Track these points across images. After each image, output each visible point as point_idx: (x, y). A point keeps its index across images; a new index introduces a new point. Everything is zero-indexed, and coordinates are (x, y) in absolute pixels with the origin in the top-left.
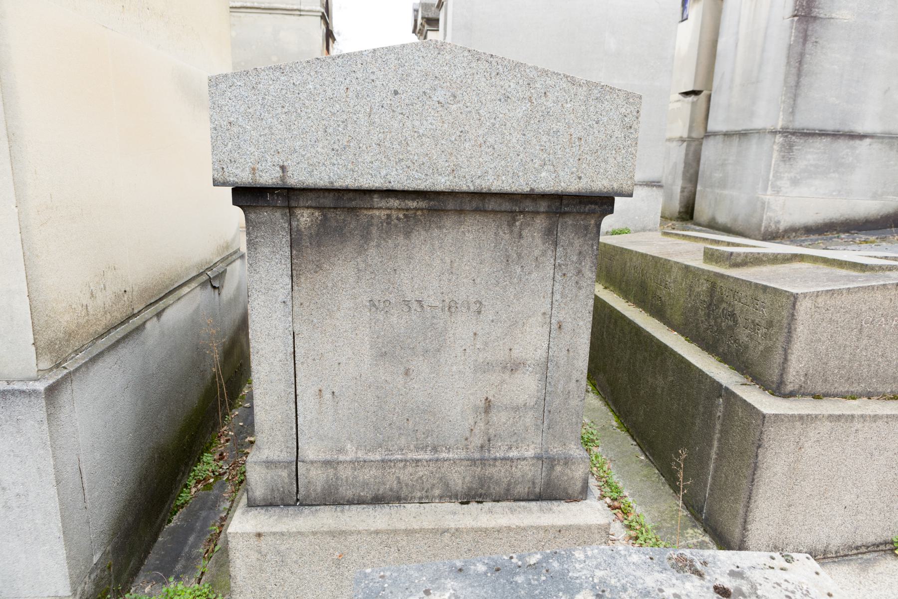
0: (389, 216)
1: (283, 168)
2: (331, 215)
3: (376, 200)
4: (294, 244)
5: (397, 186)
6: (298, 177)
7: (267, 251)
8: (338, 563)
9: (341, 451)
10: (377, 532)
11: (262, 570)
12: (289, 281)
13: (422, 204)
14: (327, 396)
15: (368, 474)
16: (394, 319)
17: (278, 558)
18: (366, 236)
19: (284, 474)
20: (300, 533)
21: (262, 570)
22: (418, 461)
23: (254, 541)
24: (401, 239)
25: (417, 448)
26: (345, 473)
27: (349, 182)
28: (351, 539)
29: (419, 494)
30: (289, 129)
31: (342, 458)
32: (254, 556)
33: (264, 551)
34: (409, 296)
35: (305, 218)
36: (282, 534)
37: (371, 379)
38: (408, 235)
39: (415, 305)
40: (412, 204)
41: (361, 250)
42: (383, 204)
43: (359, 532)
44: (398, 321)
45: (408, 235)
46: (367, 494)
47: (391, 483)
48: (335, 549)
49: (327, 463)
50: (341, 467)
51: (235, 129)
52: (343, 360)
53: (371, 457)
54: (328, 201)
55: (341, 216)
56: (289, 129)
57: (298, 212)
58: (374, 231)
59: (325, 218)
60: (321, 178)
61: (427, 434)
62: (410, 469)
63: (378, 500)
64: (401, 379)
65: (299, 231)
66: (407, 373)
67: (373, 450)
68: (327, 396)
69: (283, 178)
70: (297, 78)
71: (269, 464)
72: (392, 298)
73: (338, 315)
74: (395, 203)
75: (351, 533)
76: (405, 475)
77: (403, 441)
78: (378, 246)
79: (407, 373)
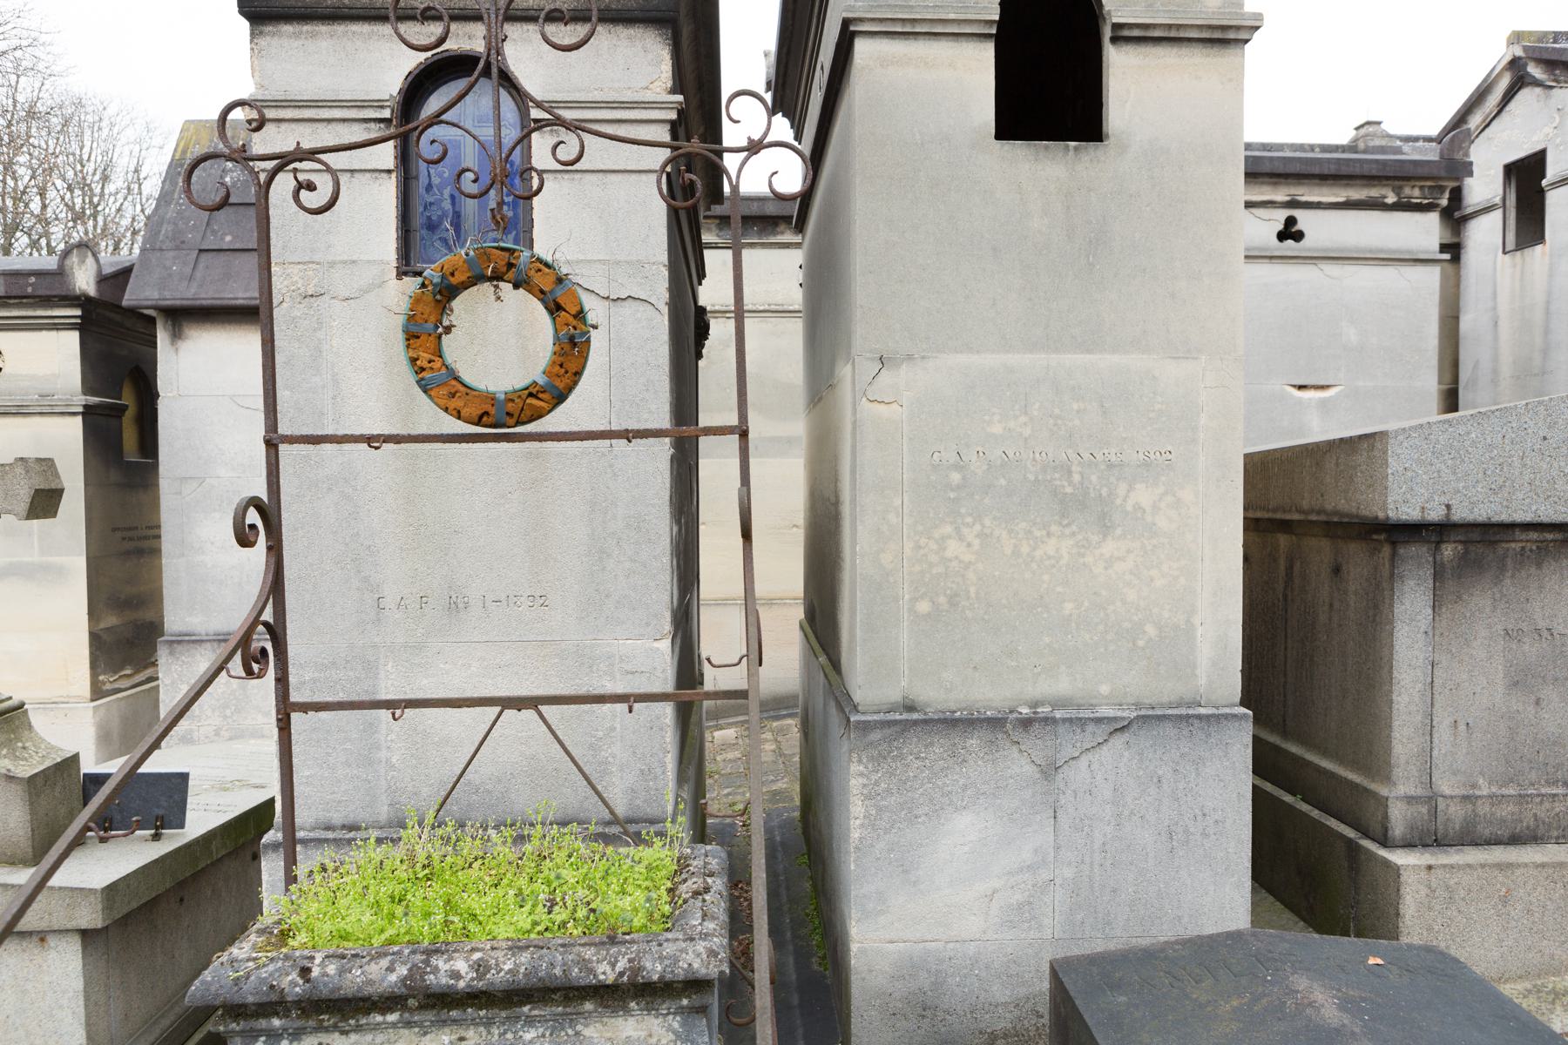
0: (1523, 548)
1: (1448, 507)
2: (1472, 548)
3: (1518, 534)
4: (1438, 575)
5: (1545, 520)
6: (1461, 514)
7: (1412, 583)
8: (1504, 900)
9: (1474, 786)
10: (1543, 865)
11: (1430, 909)
12: (1430, 611)
13: (1559, 536)
14: (1462, 727)
15: (1506, 811)
16: (1526, 647)
17: (1446, 895)
18: (1502, 568)
19: (1424, 810)
20: (1469, 866)
21: (1430, 909)
22: (1554, 795)
23: (1423, 874)
24: (1533, 570)
25: (1549, 783)
26: (1484, 809)
27: (1504, 517)
28: (1518, 872)
29: (1555, 834)
30: (1454, 473)
31: (1478, 793)
32: (1424, 891)
33: (1434, 885)
34: (1542, 624)
35: (1448, 551)
36: (1452, 867)
37: (1504, 709)
38: (1539, 565)
39: (1545, 634)
40: (1550, 536)
41: (1498, 580)
42: (1523, 537)
43: (1526, 865)
44: (1530, 649)
45: (1539, 565)
46: (1503, 833)
47: (1528, 820)
48: (1503, 884)
49: (1466, 798)
50: (1480, 802)
51: (1409, 474)
52: (1478, 690)
53: (1505, 791)
54: (1475, 536)
55: (1480, 549)
56: (1454, 473)
57: (1444, 546)
58: (1509, 561)
59: (1466, 552)
60: (1480, 514)
61: (1558, 767)
62: (1547, 805)
63: (1515, 840)
64: (1531, 709)
65: (1442, 564)
66: (1537, 702)
67: (1504, 785)
68: (1462, 727)
69: (1448, 515)
70: (1462, 430)
71: (1410, 800)
72: (1524, 626)
73: (1475, 644)
74: (1534, 535)
75: (1519, 866)
76: (1542, 811)
77: (1533, 776)
78: (1513, 576)
79: (1537, 702)
